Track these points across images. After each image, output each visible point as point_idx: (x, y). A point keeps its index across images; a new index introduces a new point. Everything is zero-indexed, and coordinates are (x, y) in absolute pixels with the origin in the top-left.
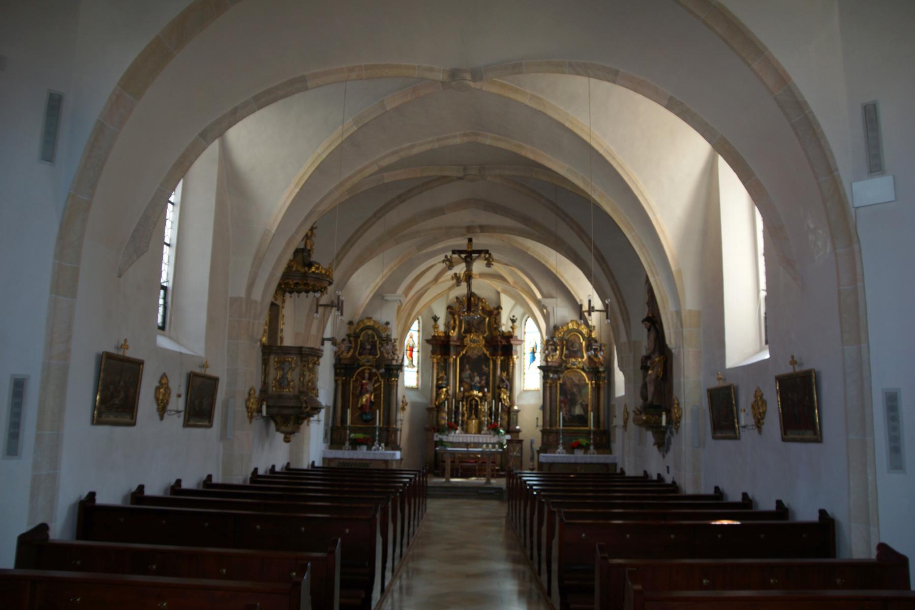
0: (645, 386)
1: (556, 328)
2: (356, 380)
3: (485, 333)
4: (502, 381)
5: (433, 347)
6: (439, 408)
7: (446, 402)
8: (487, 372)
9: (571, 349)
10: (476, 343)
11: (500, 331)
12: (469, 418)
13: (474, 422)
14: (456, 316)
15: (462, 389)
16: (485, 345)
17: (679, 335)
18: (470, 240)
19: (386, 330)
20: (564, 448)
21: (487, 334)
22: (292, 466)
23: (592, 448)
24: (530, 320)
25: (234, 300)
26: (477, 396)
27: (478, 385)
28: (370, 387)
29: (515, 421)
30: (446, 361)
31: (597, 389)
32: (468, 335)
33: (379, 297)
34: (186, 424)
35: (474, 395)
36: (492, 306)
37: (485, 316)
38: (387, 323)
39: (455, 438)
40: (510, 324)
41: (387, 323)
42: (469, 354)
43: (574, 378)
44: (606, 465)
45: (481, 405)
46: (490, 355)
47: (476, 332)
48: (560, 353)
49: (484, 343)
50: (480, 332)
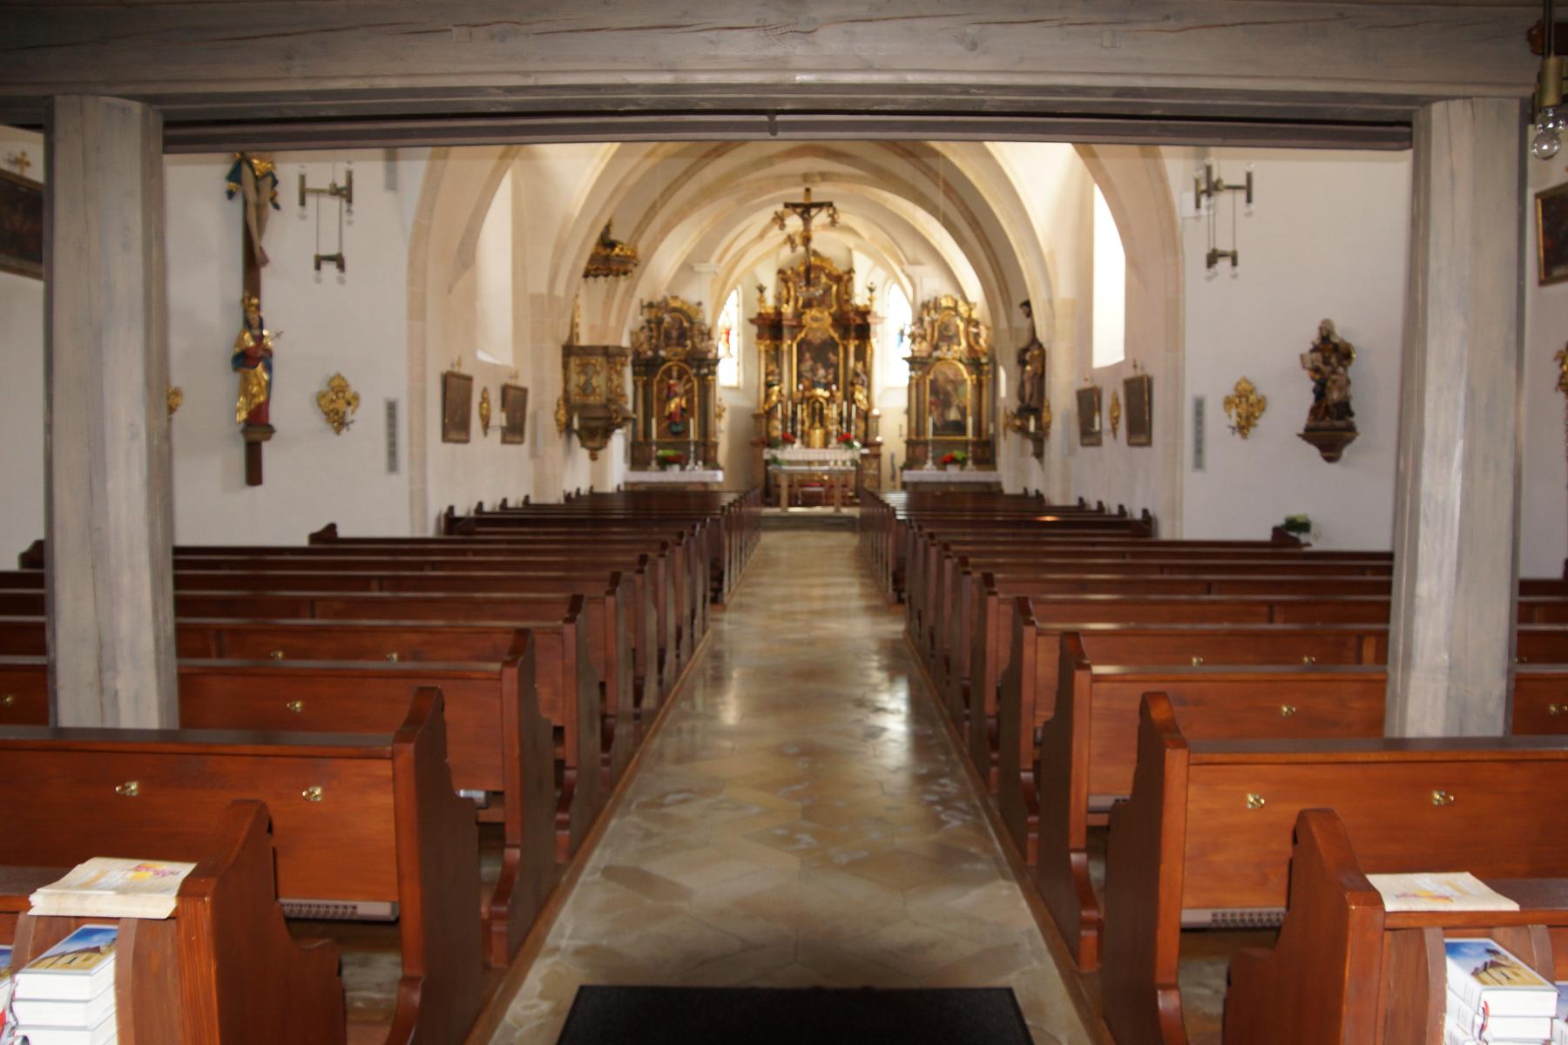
0: (1022, 385)
1: (925, 306)
2: (661, 381)
3: (831, 306)
4: (857, 375)
6: (770, 414)
7: (779, 407)
8: (836, 362)
10: (819, 323)
11: (852, 305)
12: (812, 427)
13: (818, 434)
14: (791, 285)
15: (801, 387)
17: (1051, 326)
18: (808, 190)
19: (698, 312)
20: (935, 463)
22: (597, 490)
23: (970, 463)
24: (896, 287)
25: (534, 298)
26: (822, 397)
27: (823, 381)
28: (680, 389)
29: (874, 429)
30: (777, 349)
31: (979, 386)
32: (808, 311)
33: (688, 268)
34: (504, 441)
36: (840, 268)
37: (831, 283)
38: (700, 304)
40: (868, 294)
41: (700, 304)
42: (810, 337)
44: (987, 484)
47: (819, 306)
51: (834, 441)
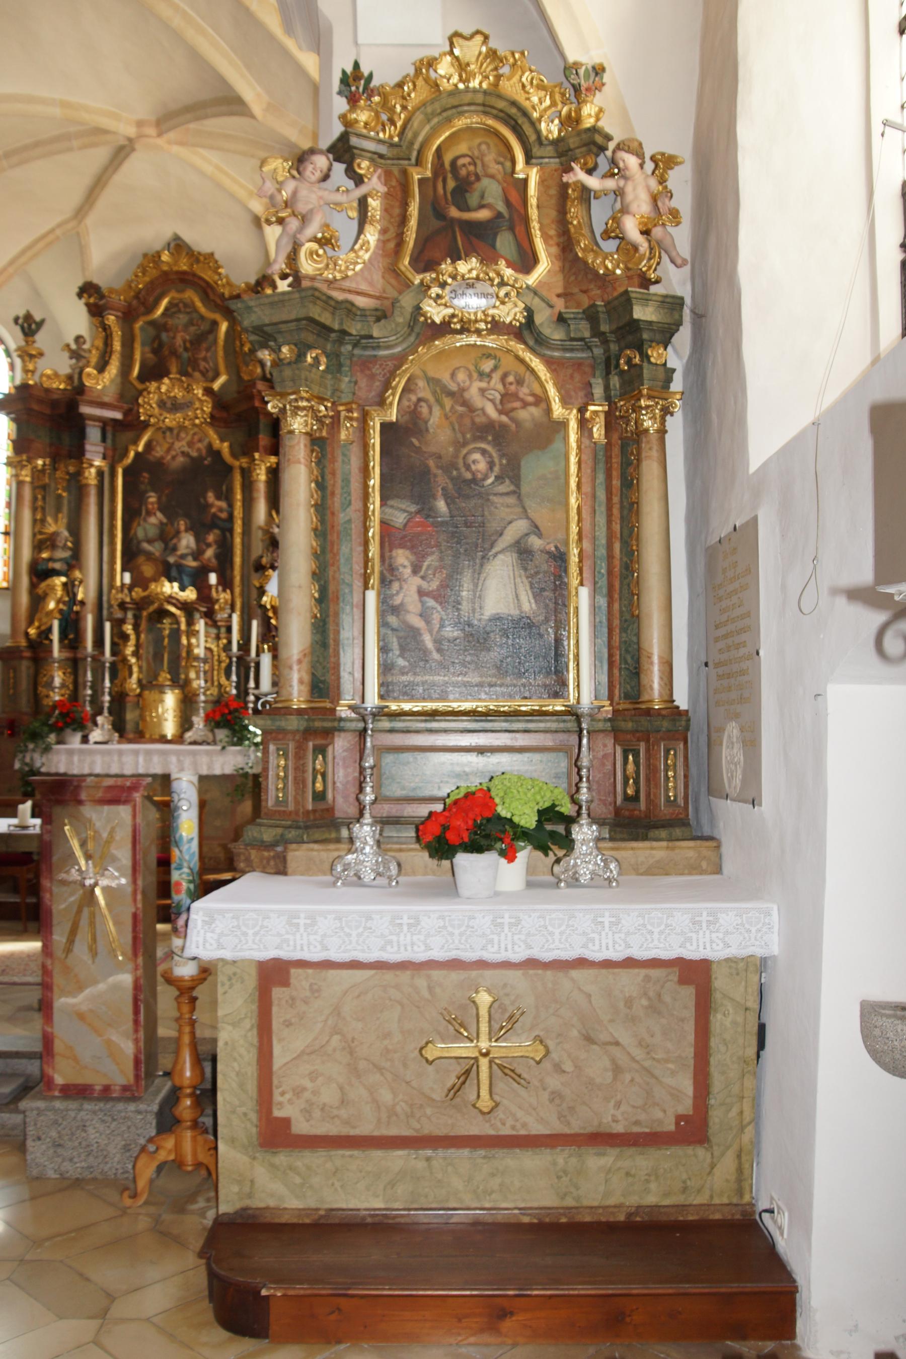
3: (217, 375)
5: (19, 430)
8: (224, 515)
9: (454, 212)
12: (150, 684)
13: (170, 700)
15: (127, 578)
16: (212, 416)
21: (222, 379)
26: (170, 599)
27: (191, 563)
32: (153, 386)
35: (163, 593)
37: (217, 317)
42: (159, 452)
43: (473, 394)
45: (192, 633)
46: (234, 455)
47: (183, 373)
48: (382, 243)
49: (208, 408)
50: (197, 375)
51: (199, 721)
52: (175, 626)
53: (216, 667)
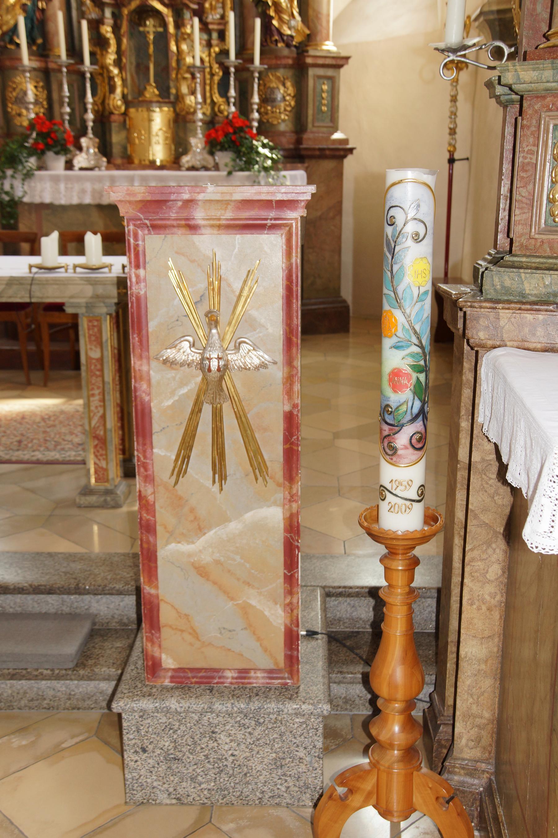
39: (62, 186)
45: (181, 37)
52: (161, 30)
53: (208, 82)
